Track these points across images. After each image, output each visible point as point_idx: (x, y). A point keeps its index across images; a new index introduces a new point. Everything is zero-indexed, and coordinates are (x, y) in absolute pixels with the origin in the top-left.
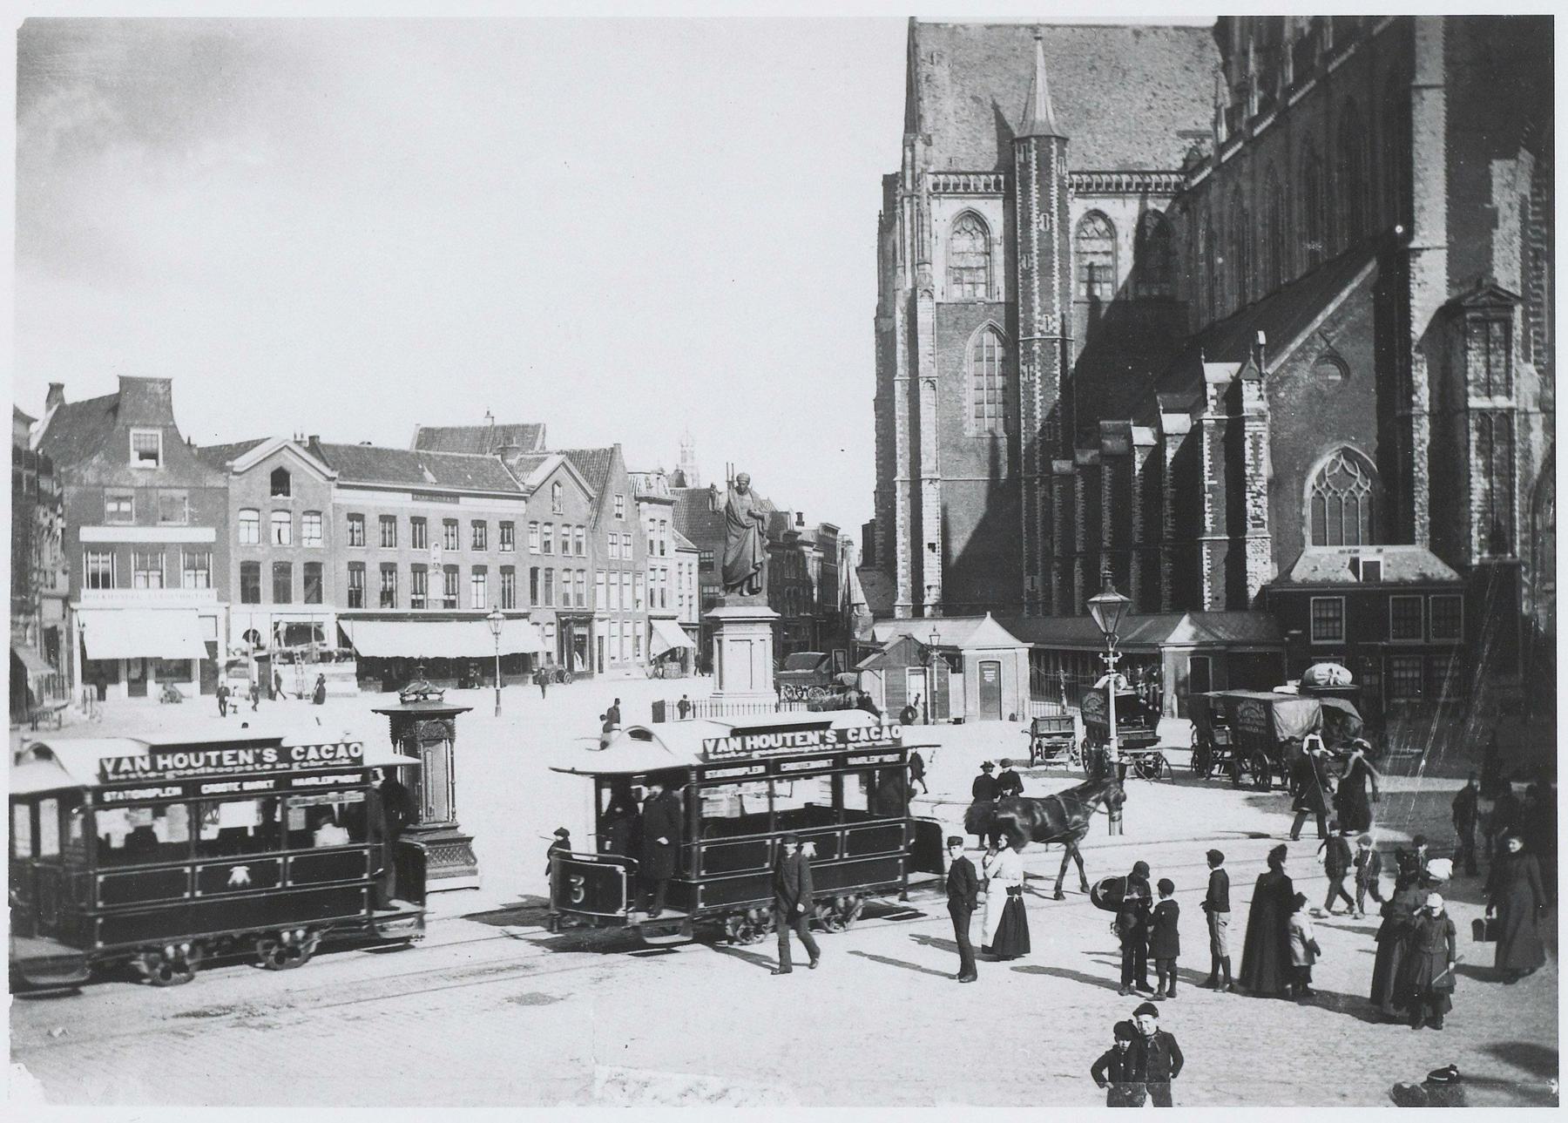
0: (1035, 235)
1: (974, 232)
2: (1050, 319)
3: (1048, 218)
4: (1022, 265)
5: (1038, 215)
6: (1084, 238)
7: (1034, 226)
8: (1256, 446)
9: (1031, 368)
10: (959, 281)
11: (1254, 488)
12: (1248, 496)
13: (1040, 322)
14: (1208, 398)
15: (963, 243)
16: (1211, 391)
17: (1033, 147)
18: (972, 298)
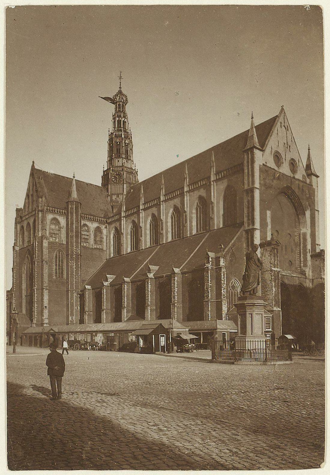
0: (74, 227)
1: (56, 224)
2: (78, 249)
3: (78, 223)
4: (70, 234)
5: (75, 222)
6: (82, 231)
7: (74, 225)
8: (224, 276)
9: (73, 262)
10: (51, 236)
11: (224, 287)
12: (222, 289)
13: (75, 250)
14: (210, 261)
15: (53, 227)
16: (210, 260)
17: (74, 204)
18: (55, 242)
